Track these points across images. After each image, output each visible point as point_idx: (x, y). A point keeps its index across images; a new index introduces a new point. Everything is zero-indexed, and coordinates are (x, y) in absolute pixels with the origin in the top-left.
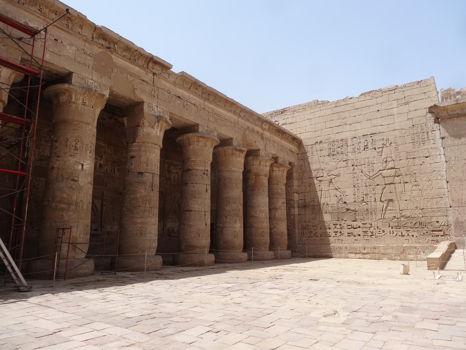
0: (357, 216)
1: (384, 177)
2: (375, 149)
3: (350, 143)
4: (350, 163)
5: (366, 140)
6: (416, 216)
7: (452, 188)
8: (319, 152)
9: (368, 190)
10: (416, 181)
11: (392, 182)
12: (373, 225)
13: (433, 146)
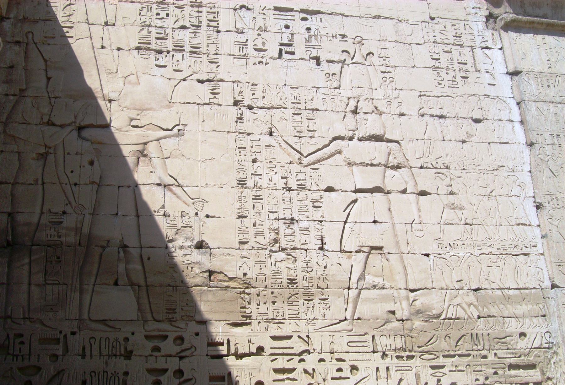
0: (253, 306)
1: (350, 165)
2: (317, 60)
3: (226, 20)
4: (227, 94)
5: (287, 27)
6: (460, 313)
7: (554, 229)
8: (97, 31)
9: (295, 202)
10: (451, 193)
11: (378, 183)
12: (315, 344)
13: (491, 91)
